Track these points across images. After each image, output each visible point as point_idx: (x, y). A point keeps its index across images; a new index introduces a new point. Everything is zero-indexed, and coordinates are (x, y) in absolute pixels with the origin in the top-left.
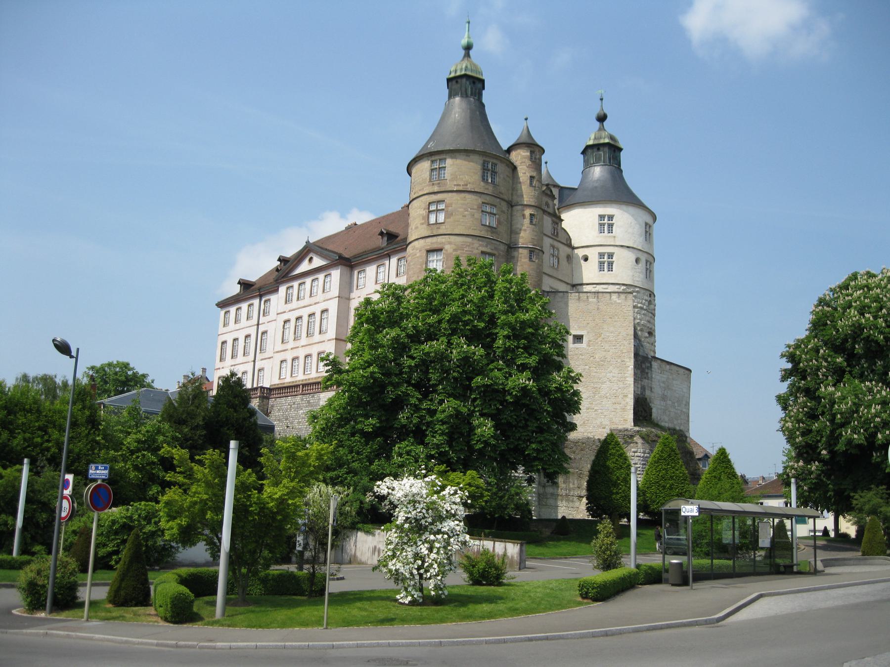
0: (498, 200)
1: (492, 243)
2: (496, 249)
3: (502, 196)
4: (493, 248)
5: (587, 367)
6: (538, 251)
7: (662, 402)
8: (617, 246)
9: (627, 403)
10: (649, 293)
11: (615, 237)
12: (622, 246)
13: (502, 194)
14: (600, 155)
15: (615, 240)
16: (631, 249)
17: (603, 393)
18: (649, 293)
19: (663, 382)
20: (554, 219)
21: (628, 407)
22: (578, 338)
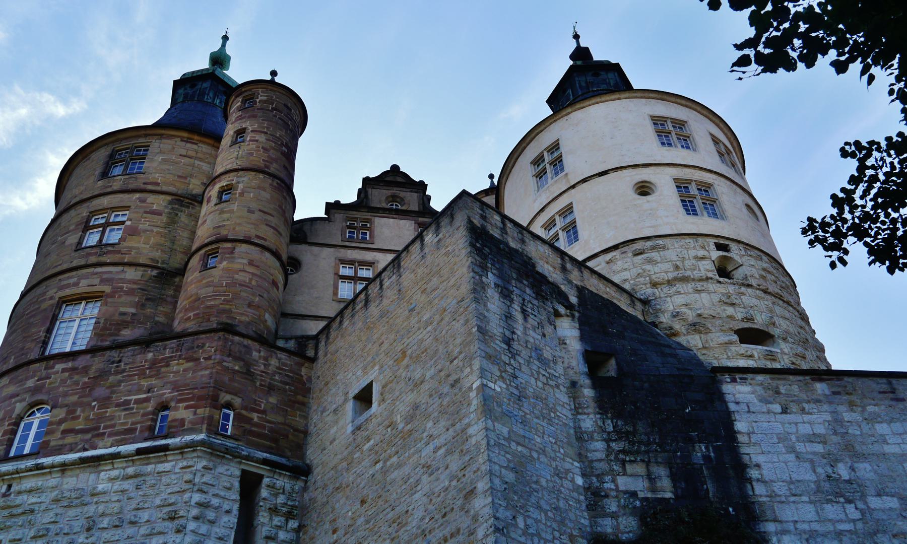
0: (137, 195)
1: (97, 273)
2: (103, 281)
3: (150, 187)
4: (97, 281)
5: (379, 466)
6: (229, 245)
7: (831, 511)
8: (573, 187)
9: (475, 519)
10: (711, 241)
11: (566, 174)
12: (584, 181)
13: (157, 184)
14: (569, 94)
15: (568, 181)
16: (612, 175)
17: (413, 522)
18: (711, 241)
19: (812, 438)
20: (420, 219)
21: (480, 533)
22: (364, 398)
